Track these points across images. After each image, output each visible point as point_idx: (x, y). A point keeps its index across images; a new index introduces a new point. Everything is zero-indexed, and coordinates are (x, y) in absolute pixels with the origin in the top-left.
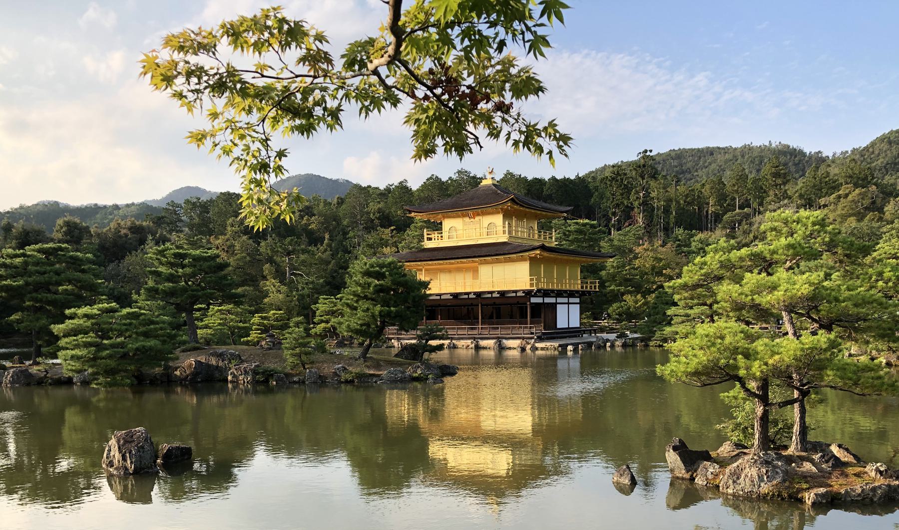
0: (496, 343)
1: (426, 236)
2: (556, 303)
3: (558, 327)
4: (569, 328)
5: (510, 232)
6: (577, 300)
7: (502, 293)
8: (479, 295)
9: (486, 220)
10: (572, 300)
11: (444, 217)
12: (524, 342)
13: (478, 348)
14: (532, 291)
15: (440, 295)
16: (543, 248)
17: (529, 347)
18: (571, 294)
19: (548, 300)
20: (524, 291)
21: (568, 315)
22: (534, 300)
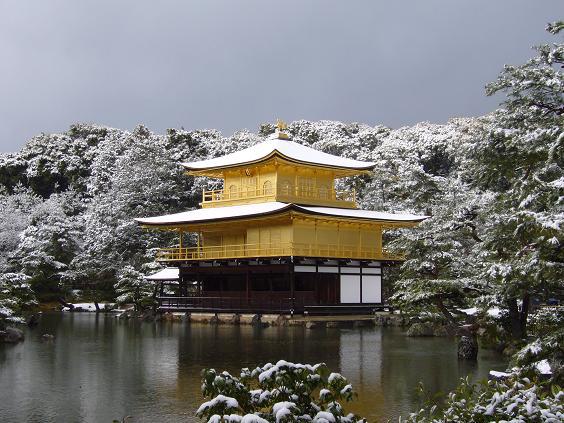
0: (254, 318)
1: (204, 196)
2: (339, 274)
4: (361, 304)
6: (378, 271)
7: (266, 261)
8: (245, 261)
9: (262, 180)
10: (365, 270)
12: (281, 318)
13: (237, 323)
15: (212, 261)
18: (364, 264)
19: (322, 270)
20: (283, 258)
22: (298, 269)
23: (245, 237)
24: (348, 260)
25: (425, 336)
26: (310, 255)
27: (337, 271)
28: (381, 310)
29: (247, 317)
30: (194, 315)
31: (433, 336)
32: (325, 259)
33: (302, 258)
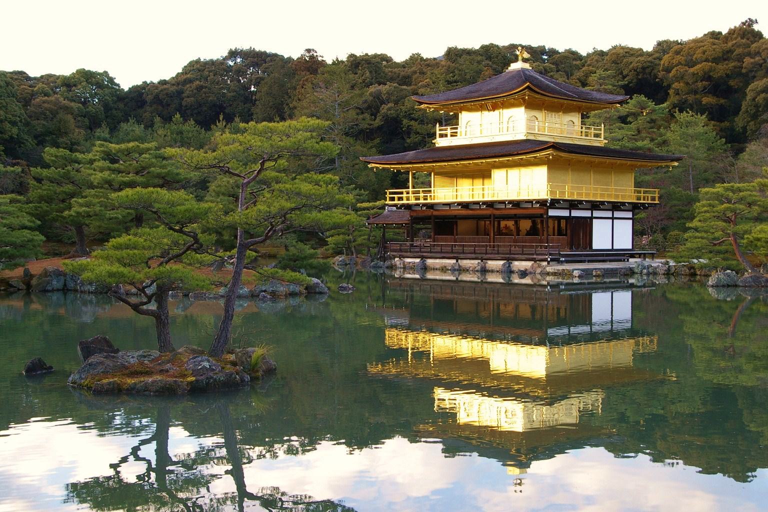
0: (504, 265)
1: (438, 132)
2: (591, 218)
3: (595, 246)
4: (613, 250)
5: (529, 127)
6: (630, 215)
7: (516, 204)
8: (490, 204)
9: (507, 113)
10: (617, 214)
11: (462, 109)
12: (536, 265)
13: (484, 271)
14: (546, 201)
15: (449, 204)
16: (556, 146)
17: (539, 270)
18: (616, 207)
19: (576, 213)
20: (538, 201)
21: (612, 234)
22: (552, 213)
23: (489, 176)
24: (602, 203)
25: (728, 286)
26: (566, 198)
27: (590, 215)
28: (632, 256)
29: (496, 264)
30: (430, 262)
31: (736, 286)
32: (581, 202)
33: (558, 201)
